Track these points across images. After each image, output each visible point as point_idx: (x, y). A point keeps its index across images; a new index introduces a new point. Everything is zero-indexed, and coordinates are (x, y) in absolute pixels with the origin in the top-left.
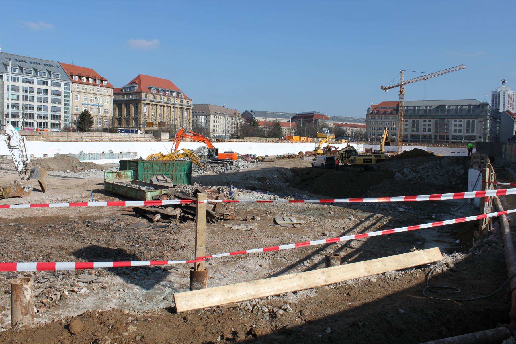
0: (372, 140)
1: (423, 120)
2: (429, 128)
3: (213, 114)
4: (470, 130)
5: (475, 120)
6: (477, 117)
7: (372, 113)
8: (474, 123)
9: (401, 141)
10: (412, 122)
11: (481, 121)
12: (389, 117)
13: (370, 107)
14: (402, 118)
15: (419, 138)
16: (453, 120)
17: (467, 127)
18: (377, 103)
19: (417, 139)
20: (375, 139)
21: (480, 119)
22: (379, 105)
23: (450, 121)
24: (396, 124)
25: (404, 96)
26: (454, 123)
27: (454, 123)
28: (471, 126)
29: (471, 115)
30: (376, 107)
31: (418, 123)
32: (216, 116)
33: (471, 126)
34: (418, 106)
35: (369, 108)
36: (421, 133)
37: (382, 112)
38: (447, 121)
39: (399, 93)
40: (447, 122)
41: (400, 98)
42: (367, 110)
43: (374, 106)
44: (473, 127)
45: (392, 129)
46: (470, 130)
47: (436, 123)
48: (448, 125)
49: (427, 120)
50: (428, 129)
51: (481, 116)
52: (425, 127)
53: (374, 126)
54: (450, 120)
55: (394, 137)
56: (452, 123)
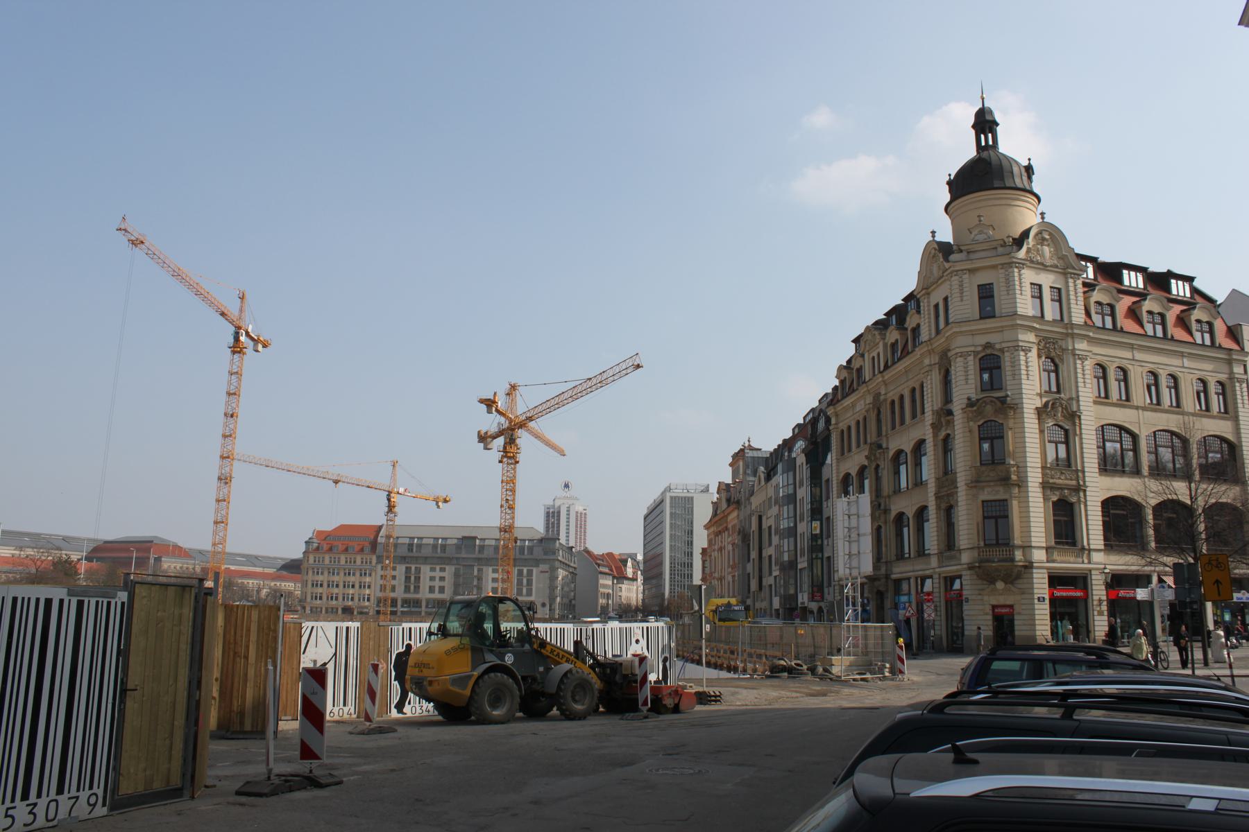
0: (314, 610)
2: (442, 584)
4: (524, 591)
6: (537, 562)
7: (317, 549)
8: (532, 576)
10: (406, 573)
12: (355, 558)
13: (311, 536)
14: (390, 563)
15: (421, 607)
17: (518, 585)
18: (329, 527)
19: (417, 609)
20: (321, 608)
22: (332, 530)
23: (484, 570)
24: (370, 575)
25: (395, 516)
26: (492, 575)
27: (492, 575)
28: (525, 581)
29: (526, 559)
30: (323, 536)
33: (525, 581)
34: (443, 539)
35: (310, 539)
36: (424, 594)
37: (341, 548)
38: (479, 570)
39: (386, 509)
40: (478, 573)
41: (387, 520)
42: (306, 542)
43: (320, 533)
44: (530, 583)
45: (360, 587)
46: (524, 591)
47: (457, 575)
48: (480, 579)
49: (438, 569)
50: (440, 587)
51: (544, 561)
52: (432, 584)
53: (320, 578)
54: (485, 568)
55: (367, 604)
56: (488, 575)
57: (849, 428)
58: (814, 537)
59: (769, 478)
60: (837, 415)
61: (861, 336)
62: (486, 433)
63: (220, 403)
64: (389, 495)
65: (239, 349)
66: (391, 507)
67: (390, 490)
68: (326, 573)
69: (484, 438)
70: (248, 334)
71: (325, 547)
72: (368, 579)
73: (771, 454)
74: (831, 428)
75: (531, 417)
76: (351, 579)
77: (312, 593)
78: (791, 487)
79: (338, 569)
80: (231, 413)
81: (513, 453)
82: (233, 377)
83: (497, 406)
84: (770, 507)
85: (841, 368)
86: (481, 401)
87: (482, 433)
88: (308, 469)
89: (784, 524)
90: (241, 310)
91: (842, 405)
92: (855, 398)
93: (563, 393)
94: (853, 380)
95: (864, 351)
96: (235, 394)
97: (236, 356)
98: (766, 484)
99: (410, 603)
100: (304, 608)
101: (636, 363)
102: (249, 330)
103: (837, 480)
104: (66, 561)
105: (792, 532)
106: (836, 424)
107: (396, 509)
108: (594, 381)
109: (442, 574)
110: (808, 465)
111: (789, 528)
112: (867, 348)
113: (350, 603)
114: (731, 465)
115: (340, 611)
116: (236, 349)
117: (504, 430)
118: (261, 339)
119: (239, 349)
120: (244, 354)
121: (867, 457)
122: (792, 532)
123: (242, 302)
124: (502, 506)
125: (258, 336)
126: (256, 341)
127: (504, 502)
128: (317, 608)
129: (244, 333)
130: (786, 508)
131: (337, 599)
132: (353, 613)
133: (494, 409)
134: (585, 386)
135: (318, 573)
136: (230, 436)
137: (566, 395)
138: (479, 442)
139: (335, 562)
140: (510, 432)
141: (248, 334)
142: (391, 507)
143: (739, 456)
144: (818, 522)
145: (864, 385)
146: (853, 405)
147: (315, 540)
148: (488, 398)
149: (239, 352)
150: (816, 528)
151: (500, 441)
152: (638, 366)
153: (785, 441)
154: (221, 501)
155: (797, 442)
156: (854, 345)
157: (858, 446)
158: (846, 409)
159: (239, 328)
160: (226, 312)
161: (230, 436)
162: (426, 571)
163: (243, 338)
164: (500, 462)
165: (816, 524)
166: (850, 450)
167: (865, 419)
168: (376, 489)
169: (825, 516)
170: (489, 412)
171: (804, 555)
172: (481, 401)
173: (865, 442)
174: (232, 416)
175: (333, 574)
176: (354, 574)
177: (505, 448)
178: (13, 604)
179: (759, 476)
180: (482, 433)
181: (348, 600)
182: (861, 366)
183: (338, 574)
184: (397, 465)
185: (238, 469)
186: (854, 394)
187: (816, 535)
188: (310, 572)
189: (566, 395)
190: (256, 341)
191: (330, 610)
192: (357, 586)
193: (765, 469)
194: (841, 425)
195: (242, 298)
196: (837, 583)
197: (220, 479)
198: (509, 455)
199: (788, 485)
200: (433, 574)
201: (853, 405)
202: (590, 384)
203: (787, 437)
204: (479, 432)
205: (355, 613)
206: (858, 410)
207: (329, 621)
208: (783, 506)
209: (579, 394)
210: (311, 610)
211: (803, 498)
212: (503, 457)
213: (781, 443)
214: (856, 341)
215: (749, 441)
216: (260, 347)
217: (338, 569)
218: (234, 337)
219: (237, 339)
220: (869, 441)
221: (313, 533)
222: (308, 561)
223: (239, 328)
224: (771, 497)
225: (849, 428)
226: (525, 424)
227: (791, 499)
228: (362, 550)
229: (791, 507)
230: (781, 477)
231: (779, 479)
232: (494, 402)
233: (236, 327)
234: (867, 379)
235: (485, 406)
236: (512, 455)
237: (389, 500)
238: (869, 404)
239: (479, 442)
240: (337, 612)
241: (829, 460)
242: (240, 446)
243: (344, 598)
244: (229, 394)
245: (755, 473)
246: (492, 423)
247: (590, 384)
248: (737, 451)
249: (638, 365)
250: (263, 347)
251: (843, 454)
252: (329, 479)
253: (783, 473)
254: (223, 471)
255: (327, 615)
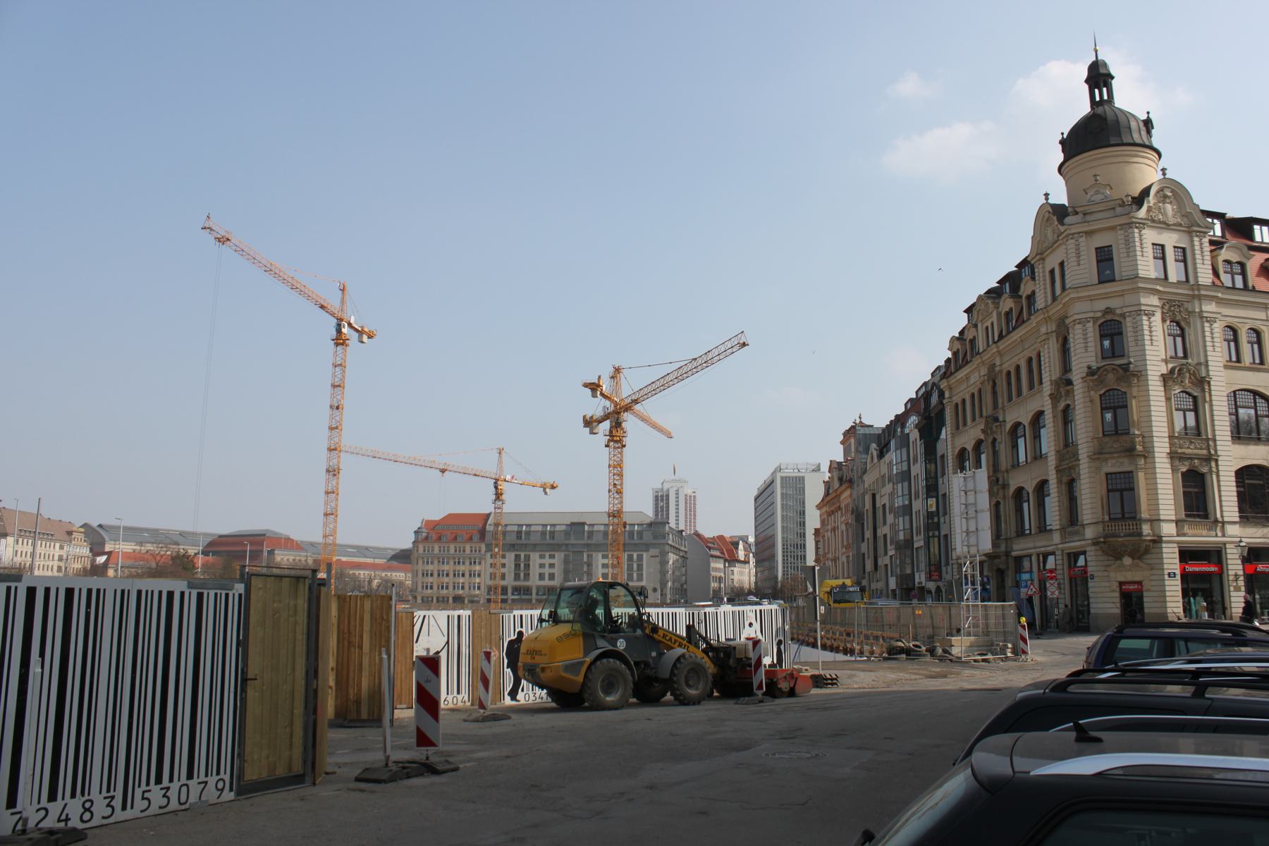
0: (425, 599)
1: (537, 555)
2: (552, 571)
3: (13, 535)
4: (635, 575)
5: (642, 555)
6: (647, 547)
7: (427, 538)
8: (642, 560)
9: (497, 602)
10: (516, 560)
11: (654, 557)
12: (464, 547)
13: (419, 526)
14: (499, 551)
15: (531, 594)
16: (600, 555)
18: (437, 516)
19: (527, 597)
20: (432, 598)
21: (653, 551)
23: (594, 556)
24: (480, 563)
25: (503, 503)
28: (635, 566)
29: (635, 544)
31: (529, 560)
32: (20, 540)
33: (635, 566)
35: (419, 528)
36: (534, 581)
39: (494, 497)
40: (588, 560)
41: (495, 508)
42: (415, 532)
44: (640, 567)
45: (470, 575)
47: (566, 562)
48: (589, 565)
49: (547, 555)
50: (550, 574)
51: (654, 546)
52: (542, 571)
53: (430, 567)
55: (477, 592)
57: (964, 401)
58: (930, 515)
59: (881, 455)
60: (951, 389)
61: (973, 305)
62: (592, 417)
63: (325, 396)
64: (496, 483)
65: (342, 341)
66: (498, 495)
67: (497, 477)
68: (436, 562)
69: (589, 423)
70: (350, 325)
71: (434, 536)
72: (477, 568)
73: (883, 430)
74: (945, 401)
75: (636, 400)
76: (461, 568)
77: (423, 583)
78: (905, 464)
79: (448, 558)
80: (336, 405)
81: (619, 436)
82: (337, 369)
83: (602, 390)
84: (884, 485)
85: (953, 339)
86: (586, 385)
87: (588, 417)
88: (415, 459)
89: (899, 502)
90: (343, 301)
91: (956, 377)
92: (970, 370)
93: (668, 374)
94: (966, 352)
95: (977, 321)
96: (339, 386)
97: (339, 348)
98: (879, 461)
99: (520, 590)
100: (415, 598)
101: (741, 342)
102: (352, 321)
103: (953, 455)
104: (184, 555)
105: (907, 510)
106: (950, 397)
107: (504, 497)
108: (700, 361)
109: (552, 561)
110: (922, 441)
111: (904, 506)
112: (980, 318)
113: (461, 592)
114: (842, 443)
115: (451, 600)
116: (339, 341)
117: (609, 414)
118: (366, 330)
119: (342, 341)
120: (347, 345)
121: (983, 431)
122: (907, 510)
123: (343, 294)
124: (609, 491)
125: (362, 327)
126: (360, 332)
127: (611, 487)
128: (428, 597)
129: (346, 325)
130: (900, 485)
131: (447, 588)
132: (464, 602)
133: (599, 393)
134: (690, 366)
135: (428, 563)
136: (337, 428)
137: (671, 377)
138: (585, 427)
139: (444, 551)
140: (616, 416)
141: (350, 325)
142: (498, 495)
143: (850, 433)
144: (934, 499)
145: (978, 356)
146: (967, 377)
147: (424, 530)
148: (592, 381)
149: (342, 344)
150: (931, 505)
151: (606, 425)
152: (744, 345)
153: (897, 416)
154: (330, 493)
155: (910, 417)
156: (966, 315)
157: (974, 419)
158: (960, 382)
159: (341, 320)
160: (325, 304)
161: (337, 428)
162: (535, 558)
163: (345, 330)
164: (607, 446)
165: (932, 501)
166: (965, 424)
167: (980, 391)
168: (482, 477)
169: (941, 493)
170: (594, 396)
171: (920, 534)
172: (586, 385)
173: (981, 416)
174: (338, 408)
175: (443, 563)
176: (464, 563)
177: (611, 432)
178: (87, 599)
179: (872, 453)
180: (588, 417)
181: (458, 588)
182: (974, 337)
183: (448, 563)
184: (503, 452)
185: (346, 462)
186: (968, 366)
187: (932, 512)
188: (420, 562)
189: (671, 377)
190: (360, 332)
191: (441, 599)
192: (467, 575)
193: (878, 446)
194: (954, 398)
195: (343, 290)
196: (955, 561)
197: (328, 471)
198: (615, 438)
199: (902, 462)
200: (542, 561)
201: (967, 377)
202: (695, 364)
203: (900, 413)
204: (584, 417)
205: (466, 601)
206: (972, 382)
207: (441, 610)
208: (898, 483)
209: (685, 375)
210: (422, 600)
211: (917, 475)
212: (609, 441)
213: (893, 418)
214: (969, 311)
215: (860, 418)
216: (365, 338)
217: (448, 558)
218: (337, 330)
219: (339, 331)
220: (984, 414)
221: (422, 523)
222: (417, 551)
223: (341, 320)
224: (884, 476)
225: (964, 401)
226: (630, 407)
227: (906, 476)
228: (471, 539)
229: (906, 484)
230: (894, 453)
231: (893, 456)
232: (599, 386)
233: (337, 319)
234: (981, 350)
235: (588, 391)
236: (618, 438)
237: (496, 488)
238: (984, 376)
239: (585, 427)
240: (448, 601)
241: (943, 436)
242: (347, 439)
243: (454, 587)
244: (334, 386)
245: (867, 450)
246: (597, 407)
247: (695, 364)
248: (847, 429)
249: (744, 343)
250: (369, 338)
251: (958, 428)
252: (436, 468)
253: (896, 449)
254: (331, 464)
255: (438, 604)
